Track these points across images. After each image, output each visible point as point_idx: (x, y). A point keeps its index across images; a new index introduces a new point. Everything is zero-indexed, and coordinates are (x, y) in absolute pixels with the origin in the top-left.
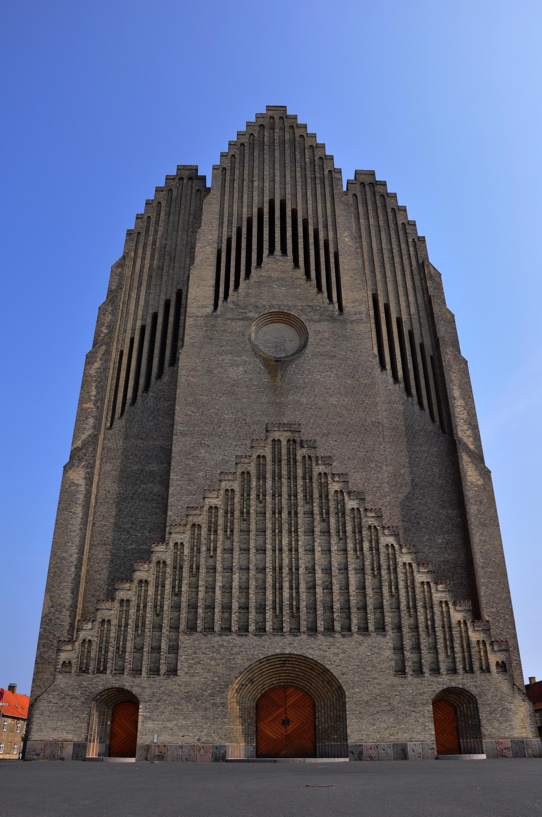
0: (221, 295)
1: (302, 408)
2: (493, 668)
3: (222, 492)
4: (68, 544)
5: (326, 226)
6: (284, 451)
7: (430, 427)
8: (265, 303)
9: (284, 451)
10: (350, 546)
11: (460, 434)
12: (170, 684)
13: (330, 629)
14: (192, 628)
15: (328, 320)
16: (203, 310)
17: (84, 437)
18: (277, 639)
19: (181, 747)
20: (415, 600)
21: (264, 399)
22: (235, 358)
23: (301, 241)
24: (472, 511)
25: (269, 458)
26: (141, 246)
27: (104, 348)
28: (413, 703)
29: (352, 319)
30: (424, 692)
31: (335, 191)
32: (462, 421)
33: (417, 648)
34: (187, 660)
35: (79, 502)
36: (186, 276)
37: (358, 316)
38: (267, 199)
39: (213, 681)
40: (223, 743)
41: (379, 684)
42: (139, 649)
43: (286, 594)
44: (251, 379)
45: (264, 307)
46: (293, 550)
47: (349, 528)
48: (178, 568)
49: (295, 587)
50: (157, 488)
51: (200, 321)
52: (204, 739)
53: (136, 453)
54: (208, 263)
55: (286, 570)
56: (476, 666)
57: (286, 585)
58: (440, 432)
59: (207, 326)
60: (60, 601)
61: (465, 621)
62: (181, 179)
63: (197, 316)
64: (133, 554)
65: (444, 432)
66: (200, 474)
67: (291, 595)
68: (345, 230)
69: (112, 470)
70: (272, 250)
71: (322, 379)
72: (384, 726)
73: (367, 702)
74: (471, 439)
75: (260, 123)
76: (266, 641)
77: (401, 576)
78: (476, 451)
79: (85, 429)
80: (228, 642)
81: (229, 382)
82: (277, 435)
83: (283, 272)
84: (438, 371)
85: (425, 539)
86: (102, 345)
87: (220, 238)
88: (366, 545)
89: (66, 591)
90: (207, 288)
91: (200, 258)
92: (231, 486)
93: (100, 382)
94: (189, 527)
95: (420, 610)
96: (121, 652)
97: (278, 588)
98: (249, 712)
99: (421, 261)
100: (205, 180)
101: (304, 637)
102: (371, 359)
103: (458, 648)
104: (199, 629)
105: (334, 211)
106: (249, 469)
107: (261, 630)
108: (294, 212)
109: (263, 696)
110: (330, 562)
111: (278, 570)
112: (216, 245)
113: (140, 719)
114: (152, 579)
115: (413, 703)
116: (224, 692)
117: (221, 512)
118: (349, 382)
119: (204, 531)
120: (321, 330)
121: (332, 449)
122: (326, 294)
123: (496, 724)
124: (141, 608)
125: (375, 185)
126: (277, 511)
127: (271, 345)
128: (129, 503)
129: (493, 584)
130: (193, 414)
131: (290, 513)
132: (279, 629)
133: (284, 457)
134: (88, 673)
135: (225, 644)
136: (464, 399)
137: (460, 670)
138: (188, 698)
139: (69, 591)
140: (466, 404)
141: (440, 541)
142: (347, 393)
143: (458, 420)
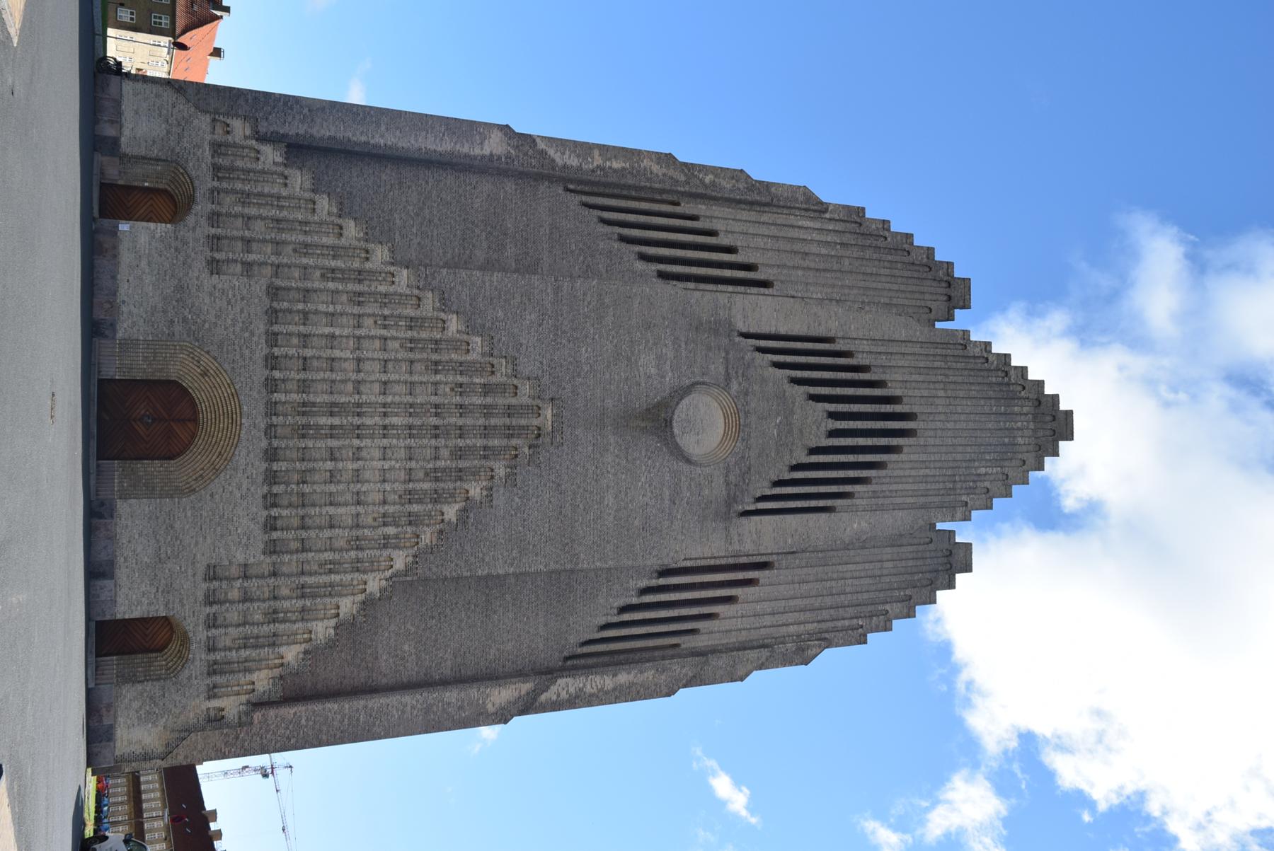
0: (763, 343)
1: (598, 456)
2: (215, 703)
3: (465, 337)
5: (875, 495)
7: (573, 639)
8: (753, 405)
10: (391, 509)
11: (561, 682)
12: (199, 264)
16: (739, 316)
17: (551, 152)
18: (261, 407)
19: (114, 278)
20: (314, 596)
21: (609, 403)
24: (448, 694)
25: (513, 401)
26: (839, 226)
27: (682, 178)
28: (168, 589)
30: (183, 605)
33: (247, 598)
34: (233, 288)
35: (458, 147)
37: (736, 538)
38: (916, 409)
39: (204, 321)
40: (120, 335)
41: (197, 543)
43: (323, 421)
47: (415, 508)
49: (333, 432)
50: (480, 255)
51: (722, 314)
52: (124, 309)
55: (357, 421)
56: (218, 679)
58: (566, 654)
60: (319, 120)
62: (949, 285)
63: (730, 309)
64: (388, 221)
66: (500, 313)
70: (832, 415)
72: (139, 550)
73: (172, 527)
74: (554, 698)
75: (1043, 400)
76: (259, 392)
78: (537, 704)
79: (563, 154)
80: (257, 344)
81: (633, 353)
82: (548, 413)
83: (801, 431)
84: (657, 653)
86: (686, 175)
88: (391, 530)
89: (333, 129)
90: (774, 323)
92: (474, 350)
94: (416, 292)
98: (161, 370)
102: (672, 554)
106: (499, 375)
109: (185, 391)
110: (367, 481)
112: (840, 335)
113: (152, 225)
115: (168, 589)
116: (189, 336)
118: (636, 522)
119: (410, 312)
122: (768, 492)
123: (136, 705)
129: (341, 722)
131: (436, 427)
134: (213, 157)
135: (255, 339)
136: (614, 689)
137: (212, 657)
138: (180, 288)
139: (332, 133)
140: (607, 693)
141: (406, 648)
142: (620, 519)
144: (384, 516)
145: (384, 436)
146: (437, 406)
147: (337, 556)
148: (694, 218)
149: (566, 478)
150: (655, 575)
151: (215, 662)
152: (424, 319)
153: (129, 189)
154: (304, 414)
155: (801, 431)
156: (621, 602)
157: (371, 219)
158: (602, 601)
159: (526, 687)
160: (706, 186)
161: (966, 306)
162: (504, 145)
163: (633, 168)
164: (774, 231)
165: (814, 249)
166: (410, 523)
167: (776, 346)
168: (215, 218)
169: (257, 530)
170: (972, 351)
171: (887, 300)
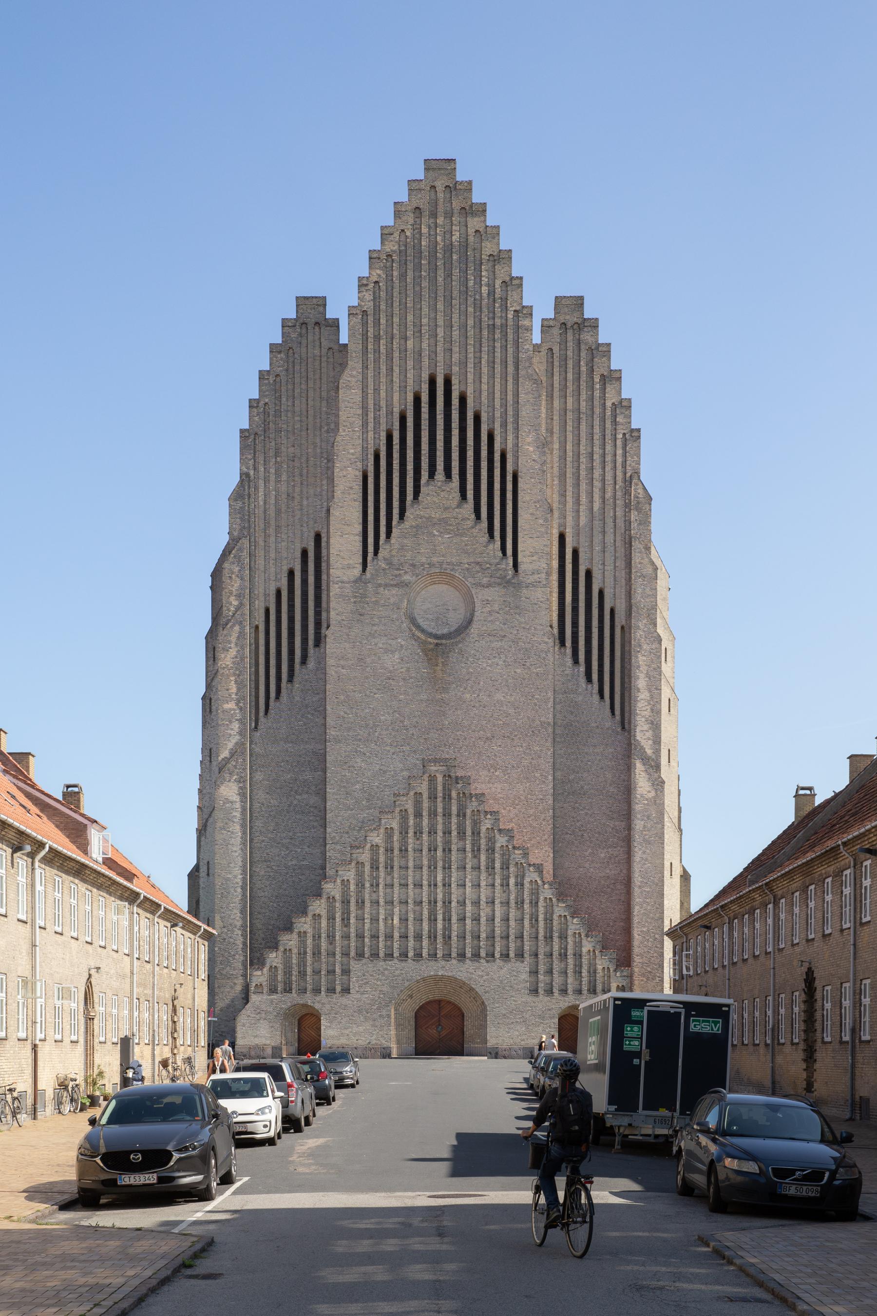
0: (371, 549)
4: (232, 865)
5: (504, 425)
6: (440, 788)
8: (424, 560)
9: (440, 788)
10: (498, 881)
11: (639, 736)
12: (344, 1000)
13: (476, 956)
14: (360, 955)
15: (499, 584)
17: (230, 745)
18: (432, 963)
20: (551, 931)
22: (390, 642)
23: (470, 463)
24: (637, 827)
26: (261, 459)
27: (237, 628)
29: (529, 581)
31: (521, 355)
32: (643, 719)
33: (550, 972)
34: (357, 981)
36: (324, 509)
37: (536, 576)
42: (317, 972)
44: (408, 670)
45: (422, 565)
46: (447, 885)
47: (498, 865)
48: (346, 902)
49: (447, 919)
50: (314, 800)
51: (348, 590)
52: (374, 1042)
53: (287, 758)
54: (351, 496)
57: (440, 917)
58: (619, 730)
59: (355, 597)
61: (594, 951)
63: (342, 582)
64: (294, 870)
65: (623, 728)
67: (444, 926)
68: (529, 432)
69: (263, 780)
71: (488, 668)
74: (650, 742)
77: (541, 910)
78: (653, 757)
79: (230, 735)
85: (587, 854)
86: (234, 625)
87: (365, 449)
88: (512, 881)
91: (342, 487)
93: (239, 675)
95: (556, 940)
96: (302, 974)
97: (433, 920)
98: (409, 1021)
99: (628, 475)
100: (338, 327)
101: (454, 962)
103: (585, 973)
104: (366, 956)
105: (516, 395)
107: (418, 955)
108: (463, 399)
109: (421, 1008)
110: (479, 897)
111: (433, 902)
114: (324, 913)
117: (382, 850)
118: (518, 671)
119: (367, 868)
120: (490, 599)
121: (495, 755)
122: (498, 543)
124: (317, 937)
125: (581, 326)
126: (433, 849)
127: (431, 617)
128: (285, 816)
130: (346, 716)
131: (444, 850)
132: (433, 956)
133: (440, 794)
138: (360, 1011)
140: (652, 697)
143: (638, 718)
144: (502, 885)
145: (450, 885)
146: (430, 850)
147: (528, 916)
148: (267, 611)
149: (481, 732)
150: (562, 649)
151: (589, 990)
152: (372, 859)
153: (299, 1040)
154: (435, 937)
155: (446, 509)
156: (583, 680)
157: (293, 882)
158: (580, 698)
159: (639, 766)
160: (241, 604)
161: (321, 302)
162: (231, 784)
163: (234, 674)
164: (272, 531)
165: (283, 488)
166: (508, 868)
167: (374, 535)
168: (317, 991)
169: (509, 966)
170: (369, 306)
171: (324, 403)
